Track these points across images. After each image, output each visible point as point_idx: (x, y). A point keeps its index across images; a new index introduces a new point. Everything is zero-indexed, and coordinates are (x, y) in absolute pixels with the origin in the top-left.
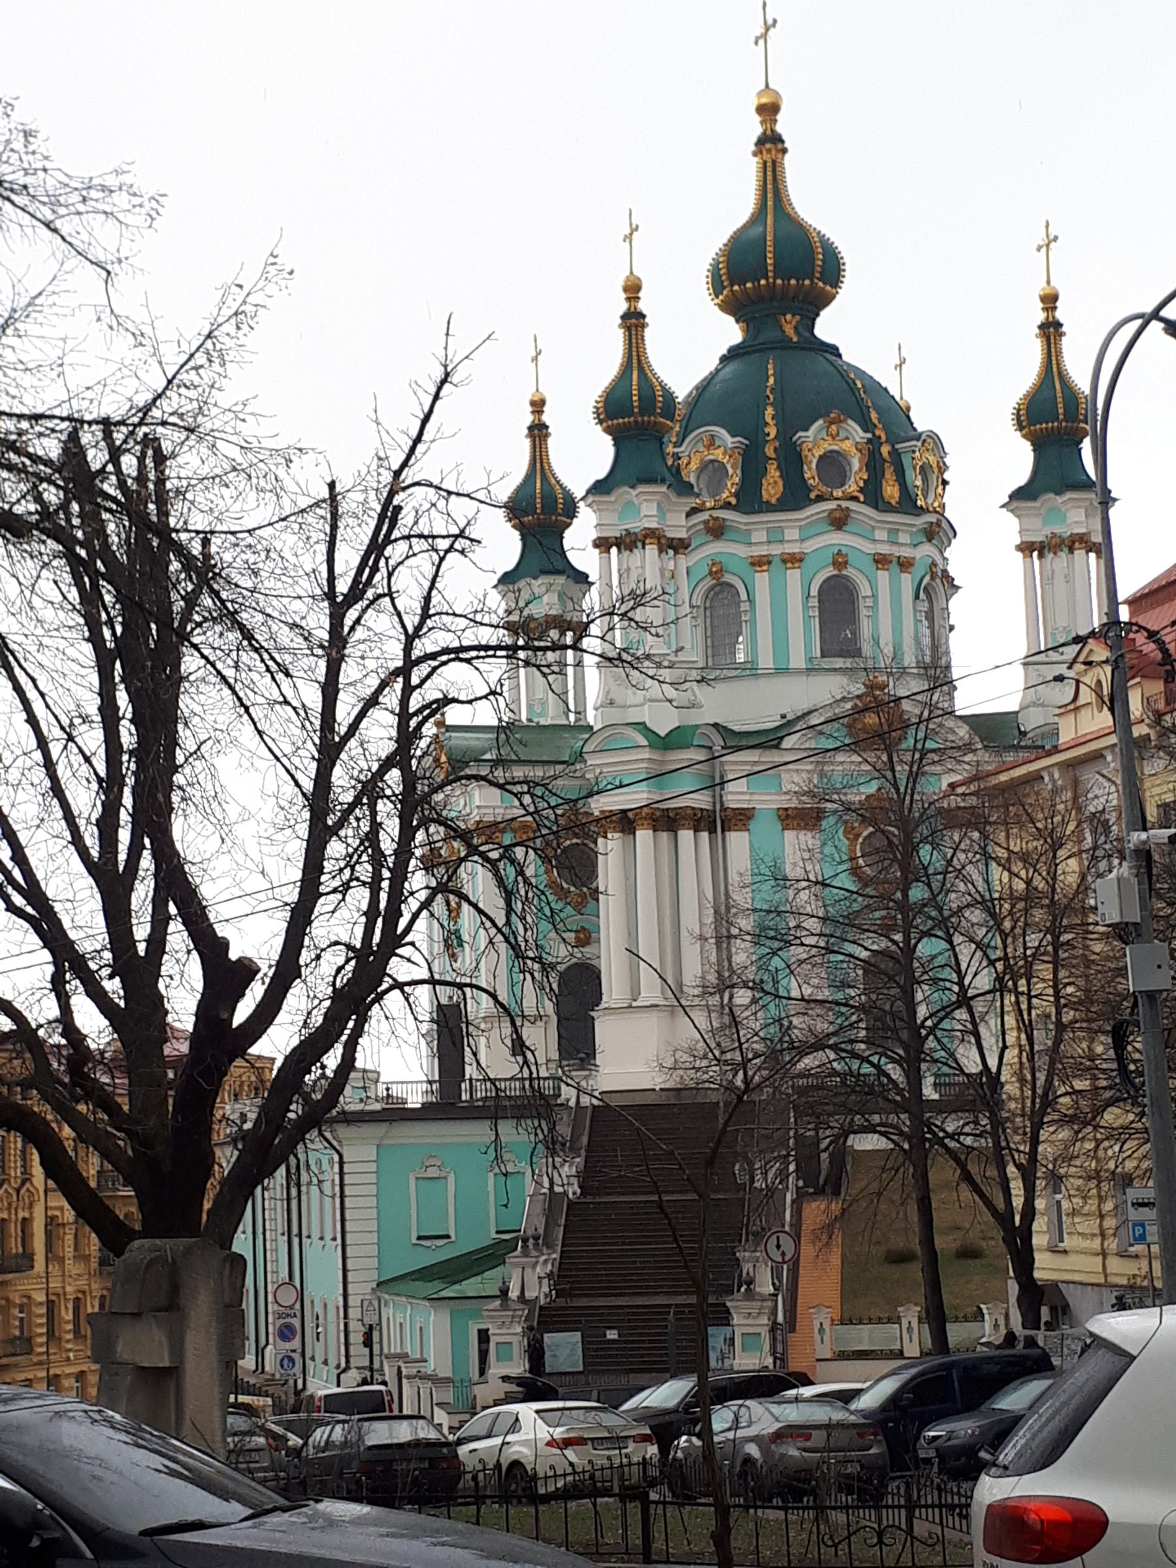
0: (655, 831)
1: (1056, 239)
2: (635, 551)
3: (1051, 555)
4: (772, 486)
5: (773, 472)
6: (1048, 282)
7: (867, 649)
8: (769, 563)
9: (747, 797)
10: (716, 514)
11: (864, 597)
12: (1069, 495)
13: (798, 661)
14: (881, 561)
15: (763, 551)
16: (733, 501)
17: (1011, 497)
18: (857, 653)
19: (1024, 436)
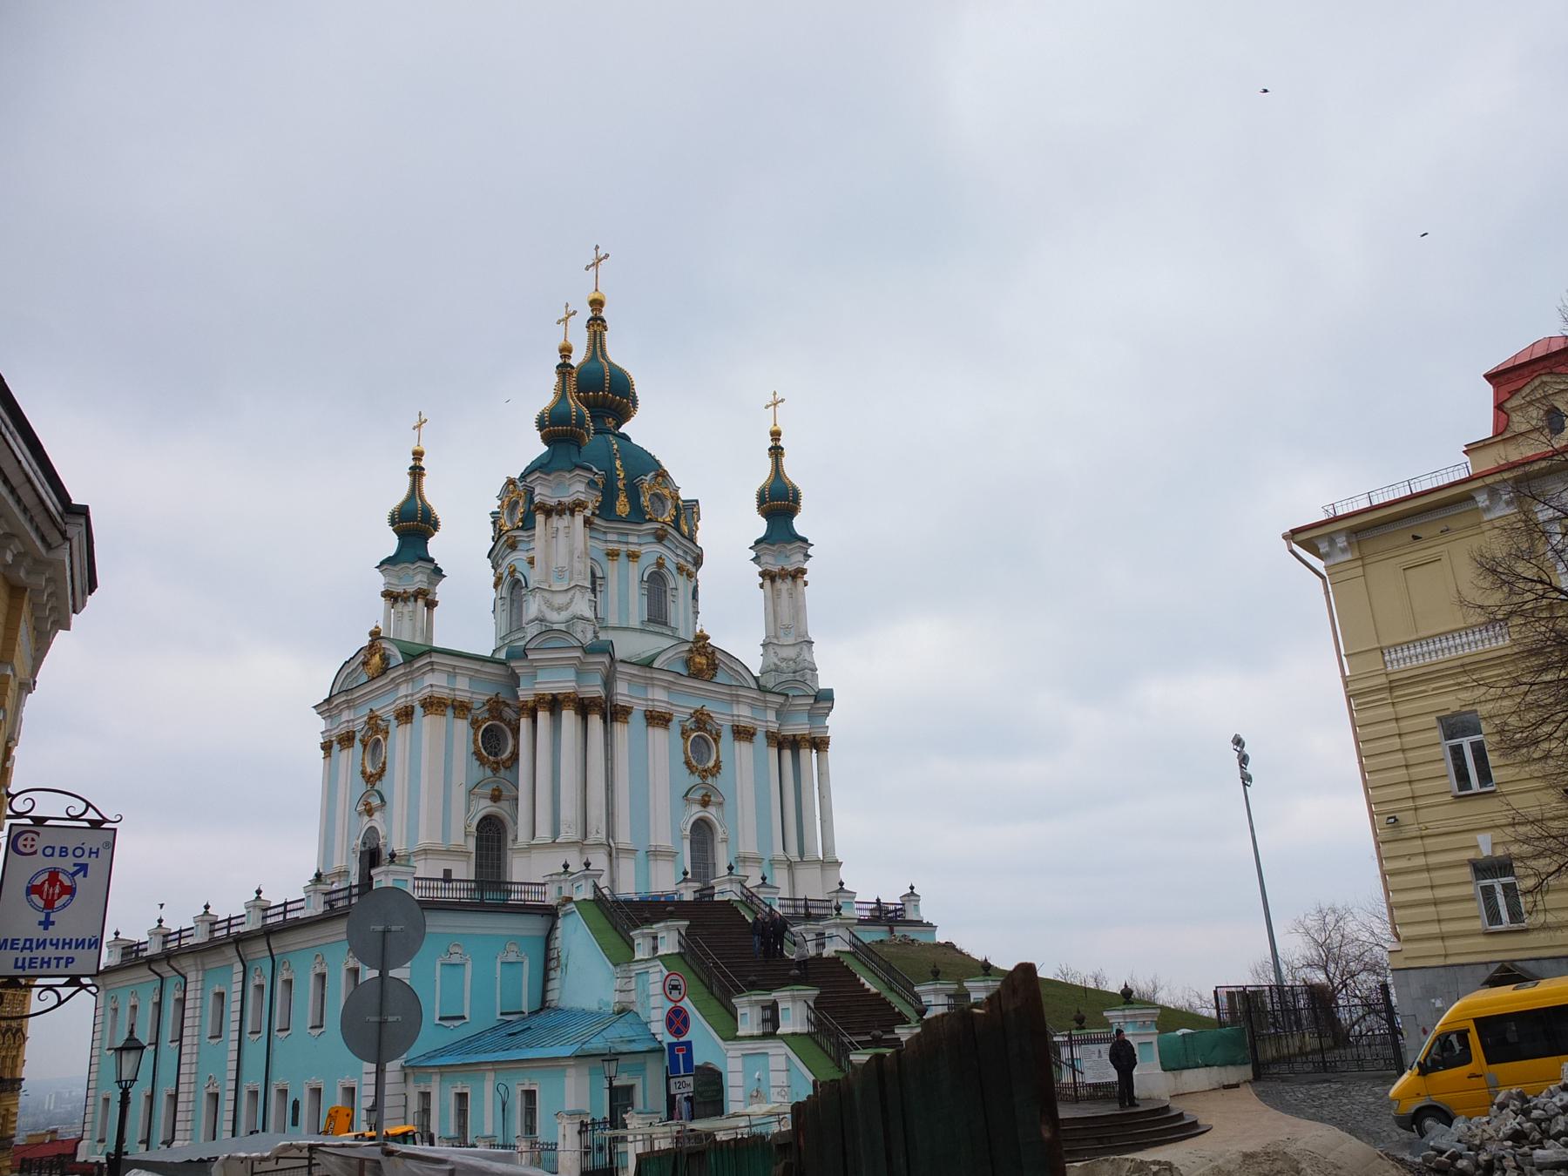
4: (622, 507)
13: (635, 622)
14: (680, 569)
17: (758, 542)
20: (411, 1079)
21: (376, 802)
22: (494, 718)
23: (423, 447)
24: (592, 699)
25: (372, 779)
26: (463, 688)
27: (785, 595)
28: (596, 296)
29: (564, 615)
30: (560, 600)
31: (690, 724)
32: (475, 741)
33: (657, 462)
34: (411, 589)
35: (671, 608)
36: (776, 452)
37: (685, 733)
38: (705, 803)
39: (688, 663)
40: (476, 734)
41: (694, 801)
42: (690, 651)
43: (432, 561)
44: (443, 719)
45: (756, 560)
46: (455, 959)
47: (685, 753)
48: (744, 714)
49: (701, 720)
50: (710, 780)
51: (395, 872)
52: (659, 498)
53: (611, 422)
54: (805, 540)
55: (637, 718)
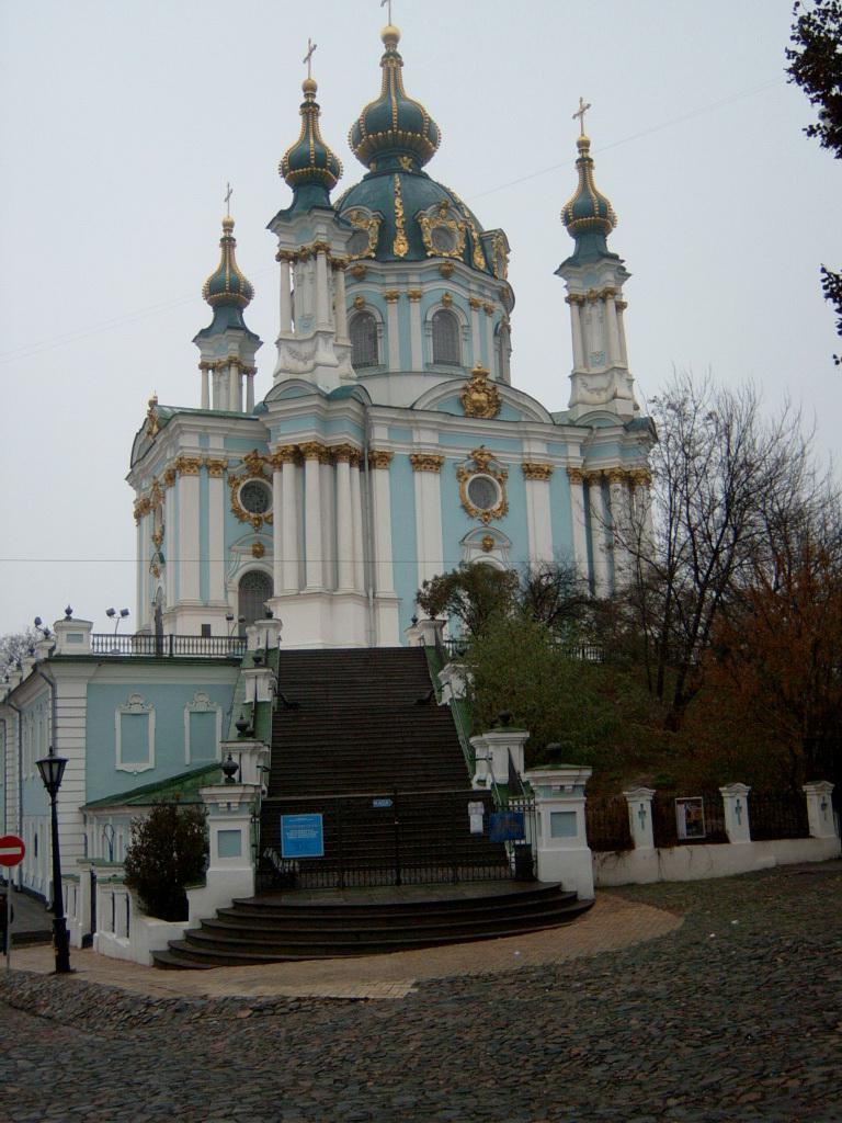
0: (320, 463)
1: (589, 106)
2: (309, 262)
3: (590, 305)
4: (401, 247)
5: (401, 237)
6: (583, 135)
7: (465, 363)
8: (397, 297)
9: (388, 444)
10: (360, 263)
11: (463, 327)
12: (606, 261)
13: (418, 365)
15: (394, 289)
16: (373, 255)
18: (458, 364)
19: (569, 230)
20: (88, 821)
21: (159, 565)
22: (254, 475)
23: (234, 217)
24: (339, 448)
25: (158, 540)
26: (217, 447)
27: (595, 321)
28: (390, 30)
29: (310, 364)
30: (306, 349)
31: (467, 465)
32: (233, 499)
33: (451, 195)
34: (224, 359)
35: (464, 347)
36: (585, 165)
37: (460, 475)
38: (487, 548)
39: (462, 401)
40: (234, 493)
41: (475, 547)
42: (465, 388)
43: (243, 328)
44: (196, 480)
45: (566, 286)
46: (136, 709)
47: (462, 496)
48: (536, 451)
49: (481, 462)
50: (494, 524)
51: (71, 628)
52: (448, 232)
53: (406, 163)
54: (615, 257)
55: (401, 465)
